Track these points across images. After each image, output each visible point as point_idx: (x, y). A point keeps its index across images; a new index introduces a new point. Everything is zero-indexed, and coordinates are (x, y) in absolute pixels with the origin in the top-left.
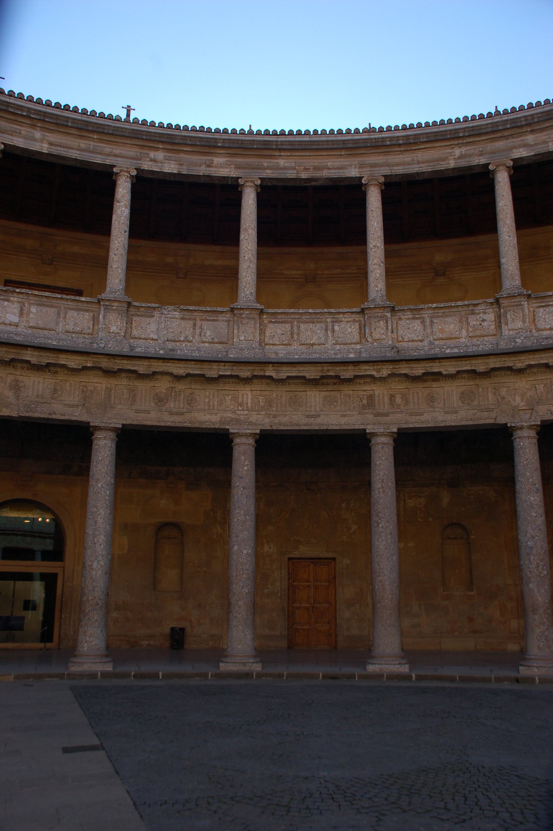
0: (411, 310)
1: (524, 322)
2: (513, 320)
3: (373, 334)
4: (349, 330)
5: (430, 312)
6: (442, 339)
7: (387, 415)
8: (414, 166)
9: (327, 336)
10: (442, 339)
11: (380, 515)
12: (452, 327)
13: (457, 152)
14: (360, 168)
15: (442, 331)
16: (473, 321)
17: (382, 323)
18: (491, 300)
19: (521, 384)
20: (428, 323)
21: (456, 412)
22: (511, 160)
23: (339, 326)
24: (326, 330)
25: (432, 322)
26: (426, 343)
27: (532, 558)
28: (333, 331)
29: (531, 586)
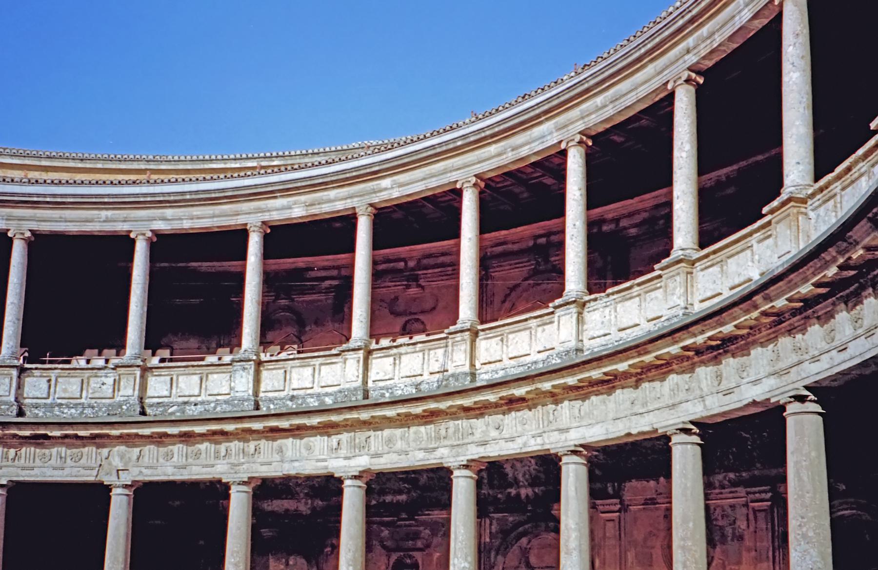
15: (65, 390)
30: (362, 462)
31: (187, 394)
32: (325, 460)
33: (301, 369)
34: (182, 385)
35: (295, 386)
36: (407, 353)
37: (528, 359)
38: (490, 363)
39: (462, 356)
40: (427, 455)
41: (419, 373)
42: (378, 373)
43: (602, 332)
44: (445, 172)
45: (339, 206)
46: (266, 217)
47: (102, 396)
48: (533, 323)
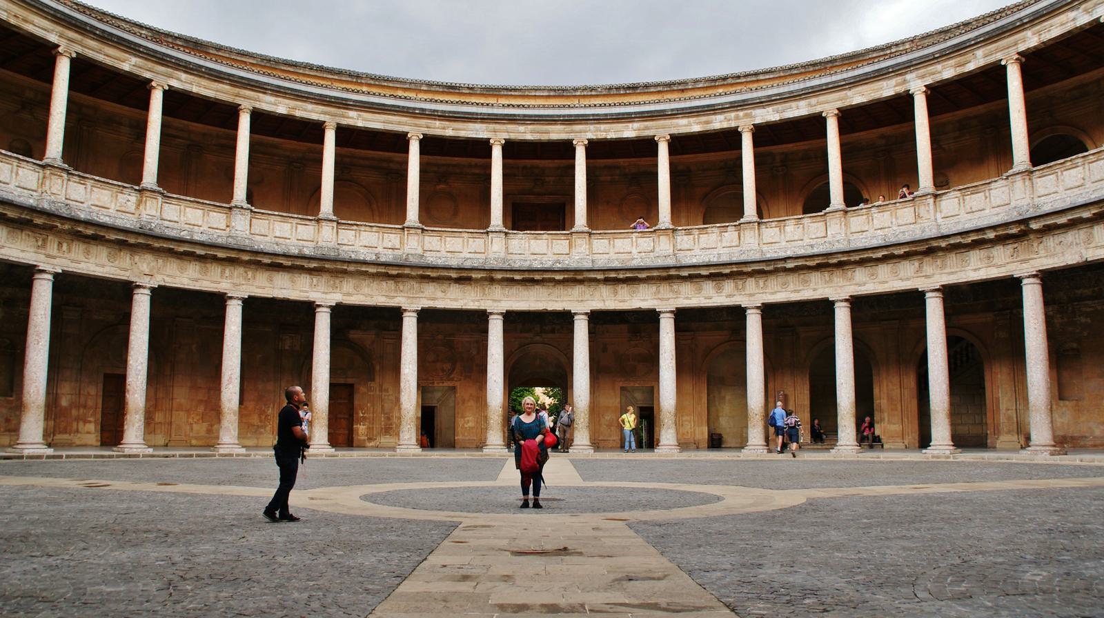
0: (79, 176)
1: (157, 212)
2: (151, 208)
3: (52, 189)
4: (30, 178)
5: (92, 182)
6: (97, 206)
7: (54, 257)
8: (100, 55)
9: (11, 176)
10: (97, 206)
11: (41, 335)
12: (106, 199)
13: (134, 60)
14: (59, 36)
15: (98, 199)
16: (122, 198)
17: (60, 181)
18: (137, 188)
19: (149, 257)
20: (89, 190)
21: (103, 266)
22: (168, 85)
23: (23, 172)
24: (12, 172)
25: (92, 190)
26: (85, 205)
27: (139, 377)
28: (17, 174)
29: (136, 395)
30: (335, 298)
31: (193, 223)
32: (307, 292)
33: (282, 223)
34: (189, 215)
35: (278, 235)
36: (365, 231)
37: (462, 255)
38: (431, 251)
39: (416, 244)
40: (388, 300)
41: (376, 246)
42: (343, 239)
43: (519, 252)
44: (399, 123)
45: (315, 117)
46: (258, 105)
47: (127, 210)
48: (466, 235)
